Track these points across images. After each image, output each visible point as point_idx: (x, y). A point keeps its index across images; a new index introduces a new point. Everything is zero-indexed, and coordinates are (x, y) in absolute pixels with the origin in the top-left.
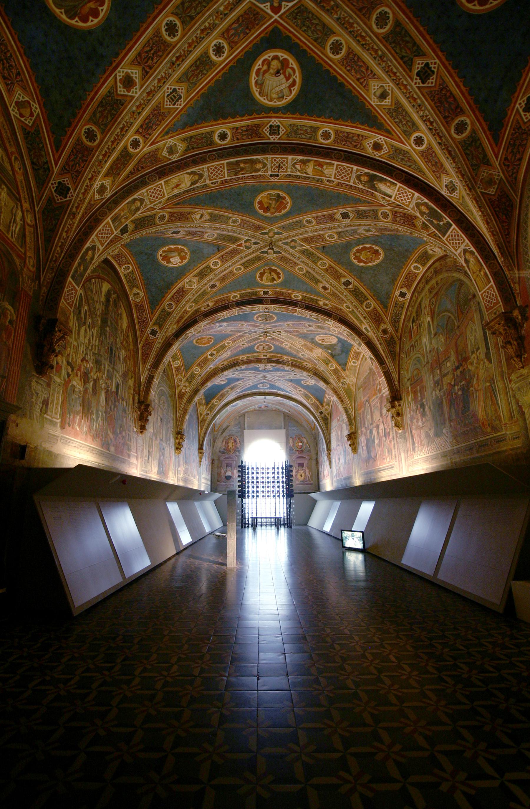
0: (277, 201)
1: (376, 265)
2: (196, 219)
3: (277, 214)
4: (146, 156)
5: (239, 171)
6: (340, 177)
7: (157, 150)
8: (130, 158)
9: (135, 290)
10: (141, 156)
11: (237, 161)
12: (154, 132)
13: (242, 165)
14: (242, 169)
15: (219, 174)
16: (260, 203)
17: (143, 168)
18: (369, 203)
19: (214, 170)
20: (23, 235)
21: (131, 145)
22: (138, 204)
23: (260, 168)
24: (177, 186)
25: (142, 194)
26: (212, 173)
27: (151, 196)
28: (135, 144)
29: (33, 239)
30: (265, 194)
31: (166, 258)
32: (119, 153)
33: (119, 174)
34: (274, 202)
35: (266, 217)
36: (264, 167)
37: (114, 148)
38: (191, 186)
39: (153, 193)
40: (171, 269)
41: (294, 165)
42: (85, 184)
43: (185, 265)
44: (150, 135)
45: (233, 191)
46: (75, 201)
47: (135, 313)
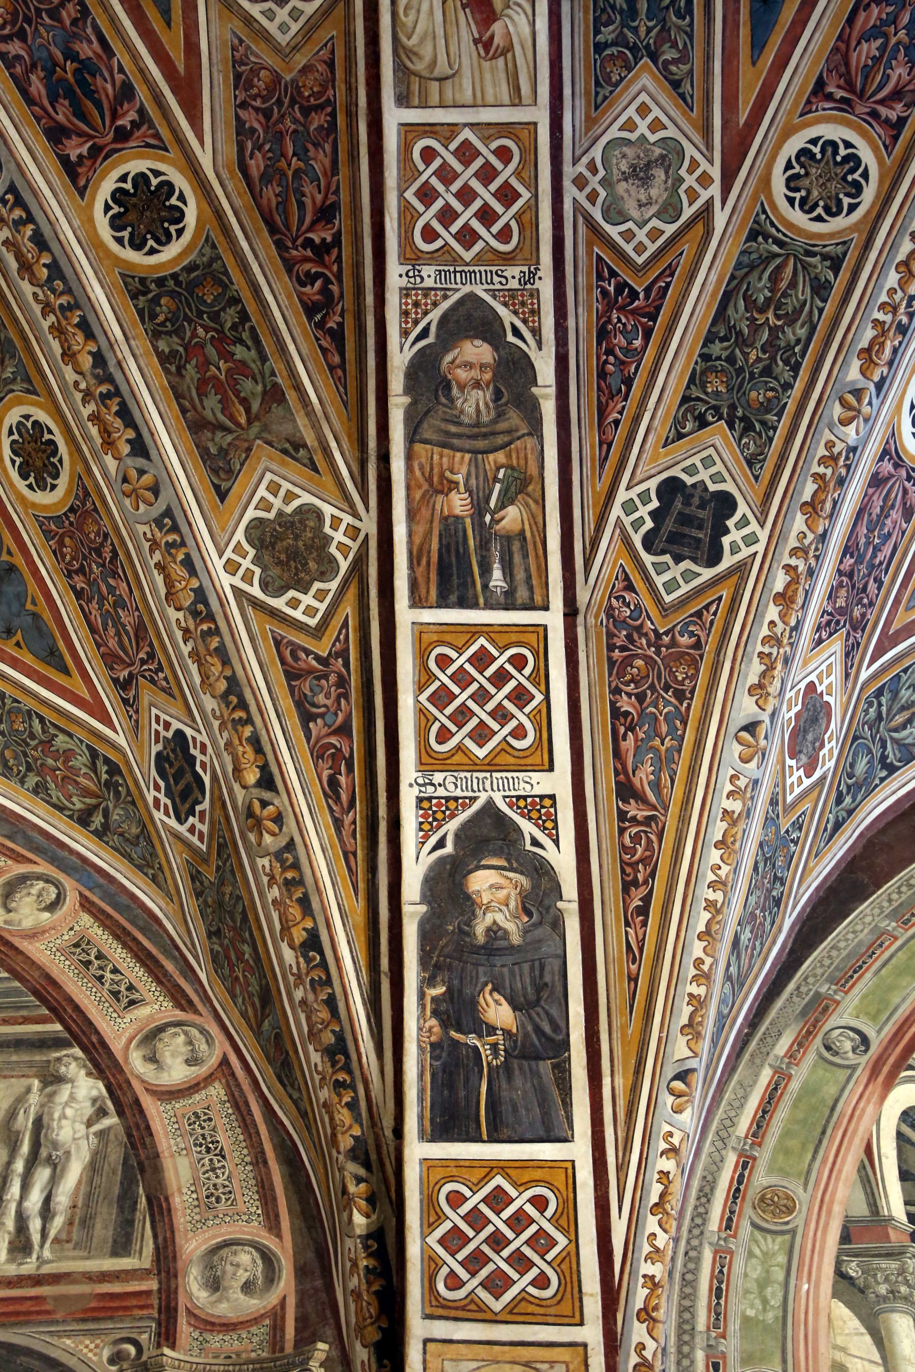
4: (256, 165)
7: (242, 76)
8: (222, 281)
10: (243, 200)
12: (121, 56)
17: (326, 213)
21: (137, 244)
22: (478, 351)
25: (416, 299)
27: (467, 237)
28: (145, 211)
32: (142, 344)
33: (274, 395)
37: (99, 359)
39: (447, 216)
42: (179, 634)
44: (127, 92)
46: (218, 756)
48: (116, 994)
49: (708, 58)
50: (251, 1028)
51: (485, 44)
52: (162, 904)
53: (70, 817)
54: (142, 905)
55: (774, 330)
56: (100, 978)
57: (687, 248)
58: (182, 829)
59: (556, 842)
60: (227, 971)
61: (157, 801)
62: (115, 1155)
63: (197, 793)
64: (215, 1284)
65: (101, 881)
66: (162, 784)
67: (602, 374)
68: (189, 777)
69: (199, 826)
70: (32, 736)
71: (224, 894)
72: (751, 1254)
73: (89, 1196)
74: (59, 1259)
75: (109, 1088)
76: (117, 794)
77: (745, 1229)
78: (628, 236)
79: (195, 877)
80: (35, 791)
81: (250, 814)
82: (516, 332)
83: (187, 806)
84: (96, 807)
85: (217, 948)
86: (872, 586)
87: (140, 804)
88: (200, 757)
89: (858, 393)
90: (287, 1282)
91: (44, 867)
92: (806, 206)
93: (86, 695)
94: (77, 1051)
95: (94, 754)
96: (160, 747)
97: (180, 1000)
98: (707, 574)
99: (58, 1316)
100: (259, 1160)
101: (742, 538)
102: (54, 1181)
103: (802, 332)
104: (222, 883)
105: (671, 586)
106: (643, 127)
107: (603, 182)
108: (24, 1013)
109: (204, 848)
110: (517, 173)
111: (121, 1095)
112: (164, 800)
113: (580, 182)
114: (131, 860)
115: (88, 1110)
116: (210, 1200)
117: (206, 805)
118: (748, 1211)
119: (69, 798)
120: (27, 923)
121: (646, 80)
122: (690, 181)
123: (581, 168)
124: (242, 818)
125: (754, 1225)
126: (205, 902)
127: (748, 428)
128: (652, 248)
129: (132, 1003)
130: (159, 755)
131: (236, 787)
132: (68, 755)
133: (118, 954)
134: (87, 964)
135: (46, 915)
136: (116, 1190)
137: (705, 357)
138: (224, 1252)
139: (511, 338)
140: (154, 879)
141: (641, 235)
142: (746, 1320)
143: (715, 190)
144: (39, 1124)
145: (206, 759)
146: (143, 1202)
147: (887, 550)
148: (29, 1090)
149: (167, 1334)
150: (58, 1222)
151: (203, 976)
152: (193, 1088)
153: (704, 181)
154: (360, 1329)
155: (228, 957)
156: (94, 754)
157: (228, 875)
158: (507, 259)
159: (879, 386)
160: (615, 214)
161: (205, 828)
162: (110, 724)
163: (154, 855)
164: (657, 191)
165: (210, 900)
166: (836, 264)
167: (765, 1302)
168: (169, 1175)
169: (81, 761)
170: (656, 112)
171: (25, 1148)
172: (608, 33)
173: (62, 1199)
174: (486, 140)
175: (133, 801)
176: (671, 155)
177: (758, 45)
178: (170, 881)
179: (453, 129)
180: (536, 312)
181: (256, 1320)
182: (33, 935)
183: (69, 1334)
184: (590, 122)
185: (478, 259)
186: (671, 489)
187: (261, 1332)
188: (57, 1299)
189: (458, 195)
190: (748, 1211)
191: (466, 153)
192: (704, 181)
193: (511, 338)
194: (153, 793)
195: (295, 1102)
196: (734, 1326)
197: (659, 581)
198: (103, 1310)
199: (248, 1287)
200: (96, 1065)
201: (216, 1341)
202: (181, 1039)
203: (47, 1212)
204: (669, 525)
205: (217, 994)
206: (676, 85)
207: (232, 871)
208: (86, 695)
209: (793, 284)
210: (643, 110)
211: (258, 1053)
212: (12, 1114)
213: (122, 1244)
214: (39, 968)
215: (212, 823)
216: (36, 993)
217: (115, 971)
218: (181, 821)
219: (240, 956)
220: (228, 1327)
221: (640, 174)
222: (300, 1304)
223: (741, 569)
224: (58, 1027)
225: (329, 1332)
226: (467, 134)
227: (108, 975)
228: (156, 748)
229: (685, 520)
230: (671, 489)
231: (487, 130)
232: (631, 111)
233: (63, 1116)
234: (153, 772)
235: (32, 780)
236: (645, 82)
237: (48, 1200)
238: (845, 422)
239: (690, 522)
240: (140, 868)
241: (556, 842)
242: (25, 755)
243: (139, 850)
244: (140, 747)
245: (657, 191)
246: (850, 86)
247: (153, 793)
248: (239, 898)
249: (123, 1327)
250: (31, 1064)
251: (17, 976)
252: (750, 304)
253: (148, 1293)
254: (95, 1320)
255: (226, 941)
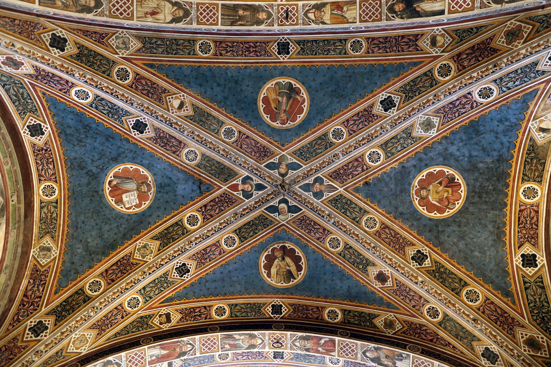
0: (289, 98)
1: (460, 212)
2: (172, 106)
3: (289, 125)
5: (237, 21)
6: (367, 18)
9: (47, 241)
11: (234, 5)
13: (241, 12)
14: (241, 18)
15: (211, 17)
16: (266, 100)
18: (415, 64)
19: (204, 11)
23: (264, 20)
24: (153, 13)
26: (201, 14)
30: (270, 84)
31: (117, 192)
34: (285, 98)
35: (273, 129)
36: (268, 18)
38: (171, 22)
40: (120, 216)
41: (306, 14)
43: (143, 214)
45: (229, 74)
47: (24, 282)
49: (143, 56)
51: (147, 13)
55: (96, 63)
57: (111, 50)
67: (88, 31)
78: (113, 40)
82: (96, 12)
86: (45, 81)
89: (85, 77)
92: (118, 71)
98: (48, 44)
101: (55, 52)
103: (96, 68)
105: (44, 36)
106: (132, 44)
107: (122, 37)
110: (125, 16)
113: (122, 32)
121: (140, 45)
122: (123, 51)
123: (125, 33)
127: (78, 56)
128: (111, 44)
137: (91, 50)
139: (95, 10)
141: (113, 42)
143: (121, 56)
147: (53, 85)
153: (123, 54)
158: (110, 12)
159: (86, 82)
160: (117, 38)
164: (121, 46)
166: (108, 75)
170: (134, 46)
172: (147, 39)
174: (131, 11)
176: (127, 48)
177: (145, 64)
179: (133, 6)
180: (100, 16)
184: (133, 35)
185: (110, 7)
186: (65, 40)
189: (121, 5)
191: (128, 8)
192: (123, 54)
193: (95, 10)
197: (46, 34)
204: (58, 39)
206: (139, 50)
209: (105, 67)
210: (135, 44)
221: (124, 43)
223: (49, 51)
226: (132, 8)
229: (59, 42)
230: (65, 40)
231: (132, 12)
232: (134, 42)
236: (139, 45)
238: (79, 74)
239: (58, 43)
245: (121, 46)
246: (138, 79)
252: (101, 60)
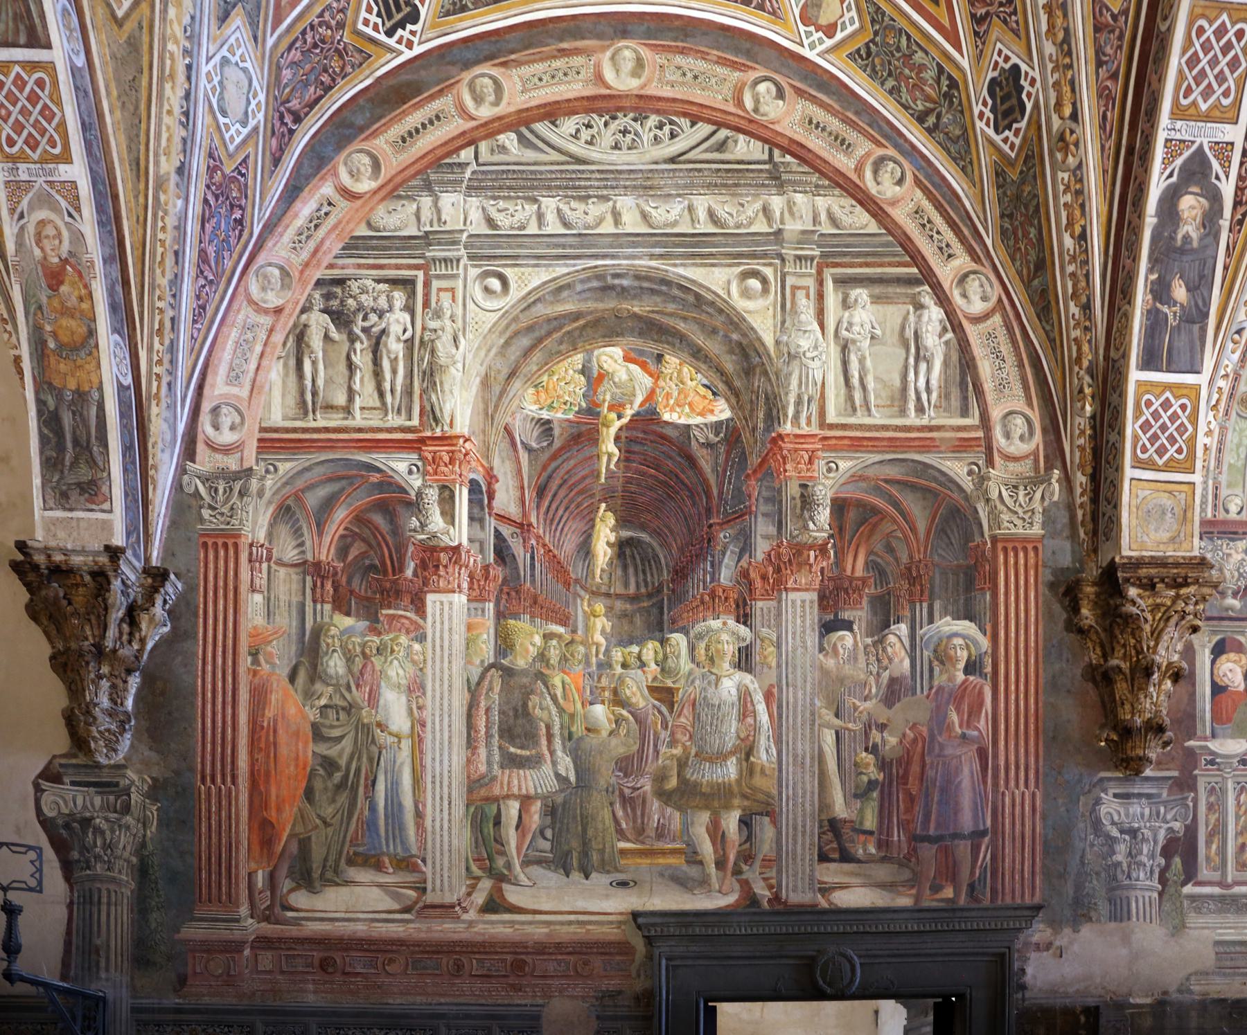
20: (964, 363)
29: (1006, 349)
48: (941, 249)
50: (1023, 281)
52: (965, 187)
53: (912, 115)
54: (949, 186)
56: (932, 237)
58: (998, 139)
59: (1227, 177)
60: (1012, 243)
61: (981, 115)
62: (955, 357)
63: (1017, 115)
64: (1007, 436)
65: (923, 164)
66: (990, 102)
68: (1014, 101)
69: (1012, 138)
70: (898, 49)
71: (1023, 191)
72: (1234, 430)
73: (946, 381)
74: (938, 417)
75: (946, 313)
76: (951, 103)
77: (1233, 415)
79: (999, 174)
80: (891, 92)
81: (1062, 138)
83: (1006, 122)
84: (932, 110)
85: (1007, 225)
87: (967, 114)
88: (1027, 87)
90: (1038, 437)
91: (891, 152)
93: (946, 22)
94: (927, 288)
95: (941, 70)
96: (996, 74)
97: (975, 258)
99: (943, 449)
100: (1021, 365)
102: (929, 370)
104: (1023, 182)
108: (897, 259)
109: (1013, 155)
111: (953, 321)
112: (988, 113)
114: (949, 152)
115: (939, 328)
116: (1001, 386)
117: (1023, 124)
118: (1235, 406)
119: (914, 101)
120: (889, 194)
124: (1054, 140)
125: (1238, 414)
126: (1005, 193)
129: (950, 256)
130: (993, 80)
131: (1055, 117)
132: (922, 68)
133: (938, 220)
134: (924, 226)
135: (898, 188)
136: (958, 378)
138: (1010, 417)
140: (963, 169)
142: (1230, 465)
144: (916, 333)
145: (1033, 91)
146: (970, 385)
148: (908, 313)
149: (990, 462)
150: (934, 396)
151: (989, 242)
152: (986, 316)
154: (1081, 466)
155: (1015, 233)
156: (941, 70)
157: (1030, 178)
161: (1017, 142)
162: (958, 47)
163: (968, 152)
165: (1009, 193)
167: (1238, 456)
168: (981, 370)
169: (929, 75)
171: (913, 350)
173: (934, 383)
175: (962, 110)
178: (976, 172)
181: (1027, 457)
182: (894, 203)
183: (949, 459)
187: (1029, 462)
188: (942, 439)
190: (1235, 406)
194: (980, 107)
195: (1047, 333)
196: (1225, 468)
198: (962, 446)
199: (1022, 438)
200: (938, 298)
201: (1012, 466)
202: (977, 283)
203: (928, 390)
205: (1000, 257)
207: (1035, 177)
208: (946, 22)
211: (1024, 297)
212: (903, 328)
213: (965, 412)
214: (900, 227)
215: (1024, 138)
216: (901, 245)
217: (938, 233)
218: (997, 131)
219: (1026, 234)
220: (1016, 459)
222: (1045, 449)
224: (915, 270)
225: (1059, 464)
227: (936, 236)
228: (991, 75)
233: (927, 331)
234: (985, 92)
235: (890, 83)
237: (928, 382)
240: (954, 159)
241: (1227, 177)
242: (890, 63)
243: (957, 147)
244: (979, 72)
247: (980, 106)
248: (1036, 196)
249: (969, 456)
250: (907, 295)
251: (890, 233)
253: (979, 439)
254: (959, 452)
255: (1017, 223)
